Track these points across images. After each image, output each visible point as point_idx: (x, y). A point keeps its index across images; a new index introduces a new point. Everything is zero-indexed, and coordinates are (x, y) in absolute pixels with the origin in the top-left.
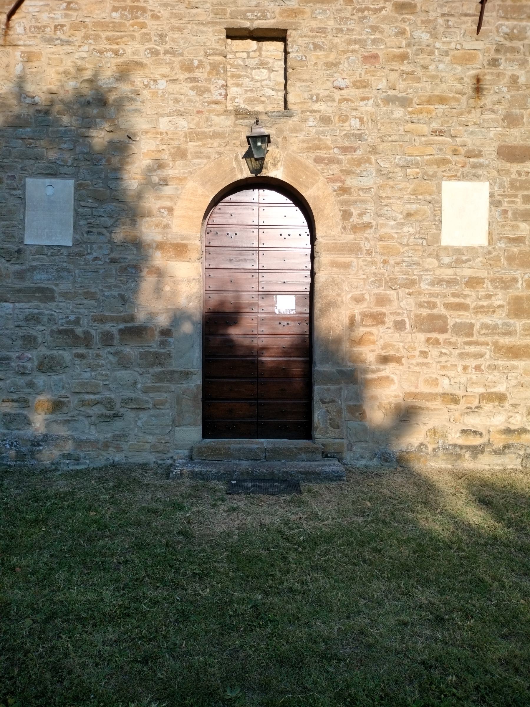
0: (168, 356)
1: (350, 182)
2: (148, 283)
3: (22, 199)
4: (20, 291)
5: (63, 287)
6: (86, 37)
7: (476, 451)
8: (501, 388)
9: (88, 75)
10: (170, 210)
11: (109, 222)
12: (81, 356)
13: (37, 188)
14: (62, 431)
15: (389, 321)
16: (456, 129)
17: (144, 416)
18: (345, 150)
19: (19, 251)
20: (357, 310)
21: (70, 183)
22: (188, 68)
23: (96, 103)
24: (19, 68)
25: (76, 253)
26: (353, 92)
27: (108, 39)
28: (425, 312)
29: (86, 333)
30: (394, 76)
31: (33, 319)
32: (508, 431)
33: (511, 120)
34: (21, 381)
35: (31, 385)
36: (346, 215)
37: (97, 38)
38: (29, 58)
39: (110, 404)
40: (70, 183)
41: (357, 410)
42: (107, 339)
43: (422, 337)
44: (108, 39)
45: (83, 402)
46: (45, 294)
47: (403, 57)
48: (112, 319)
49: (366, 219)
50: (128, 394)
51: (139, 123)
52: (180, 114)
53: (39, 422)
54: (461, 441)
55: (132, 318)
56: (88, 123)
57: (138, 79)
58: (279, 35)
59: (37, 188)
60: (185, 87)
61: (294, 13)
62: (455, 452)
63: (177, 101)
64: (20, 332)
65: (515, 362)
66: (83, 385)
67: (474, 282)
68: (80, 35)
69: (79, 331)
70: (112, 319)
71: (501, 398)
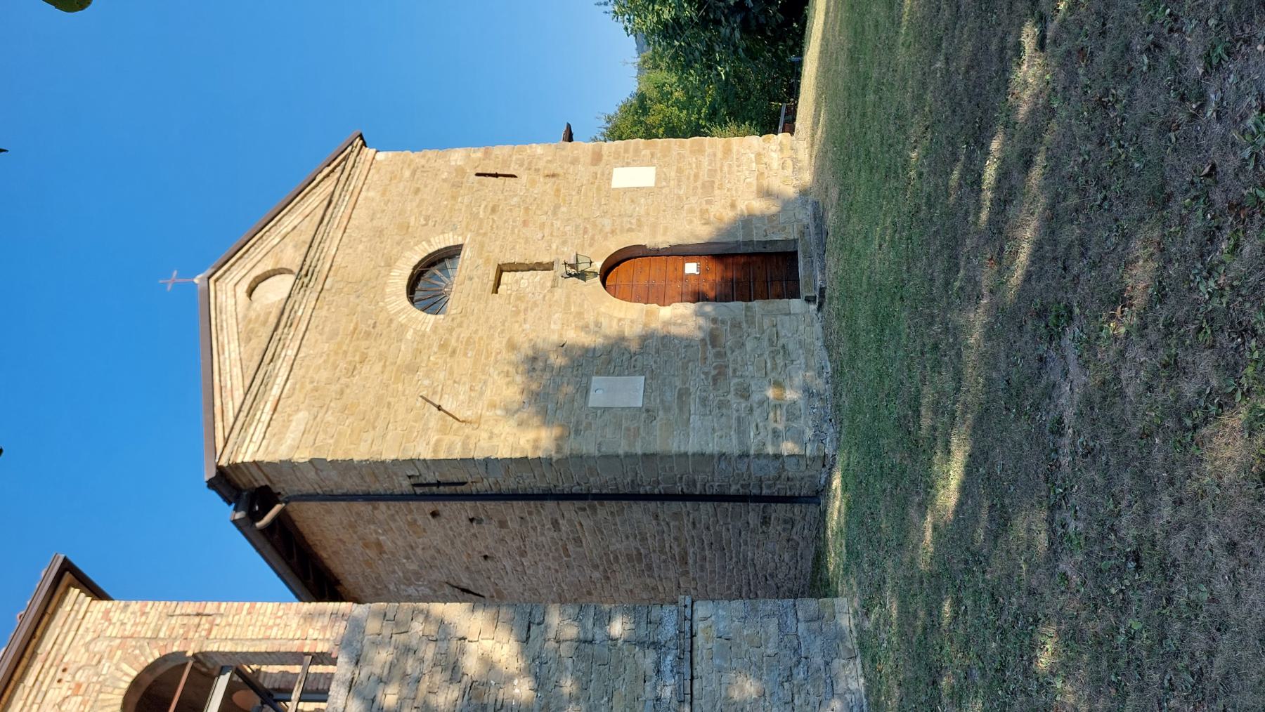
0: (734, 319)
1: (608, 229)
2: (674, 330)
3: (605, 410)
4: (681, 409)
5: (678, 384)
6: (483, 372)
7: (795, 161)
8: (753, 156)
9: (512, 370)
10: (620, 320)
11: (627, 356)
12: (735, 371)
13: (597, 398)
14: (798, 380)
15: (705, 207)
16: (578, 183)
17: (782, 333)
18: (585, 232)
19: (648, 411)
20: (697, 222)
21: (594, 378)
22: (517, 313)
23: (534, 362)
24: (499, 412)
25: (651, 375)
26: (547, 231)
27: (487, 358)
28: (700, 191)
29: (715, 368)
30: (539, 212)
31: (704, 401)
32: (781, 150)
33: (575, 161)
34: (757, 412)
35: (761, 403)
36: (630, 230)
37: (485, 365)
38: (493, 406)
39: (774, 355)
40: (594, 378)
41: (771, 218)
42: (719, 355)
43: (717, 192)
44: (487, 358)
45: (774, 368)
46: (683, 394)
47: (527, 209)
48: (704, 352)
49: (634, 221)
50: (765, 343)
51: (555, 338)
52: (549, 317)
53: (791, 395)
54: (791, 170)
55: (703, 340)
56: (547, 367)
57: (520, 339)
58: (501, 270)
59: (597, 398)
60: (531, 315)
61: (487, 260)
62: (797, 169)
63: (540, 318)
64: (716, 411)
65: (734, 151)
66: (759, 370)
67: (680, 170)
68: (479, 375)
69: (714, 372)
70: (704, 352)
71: (759, 155)
